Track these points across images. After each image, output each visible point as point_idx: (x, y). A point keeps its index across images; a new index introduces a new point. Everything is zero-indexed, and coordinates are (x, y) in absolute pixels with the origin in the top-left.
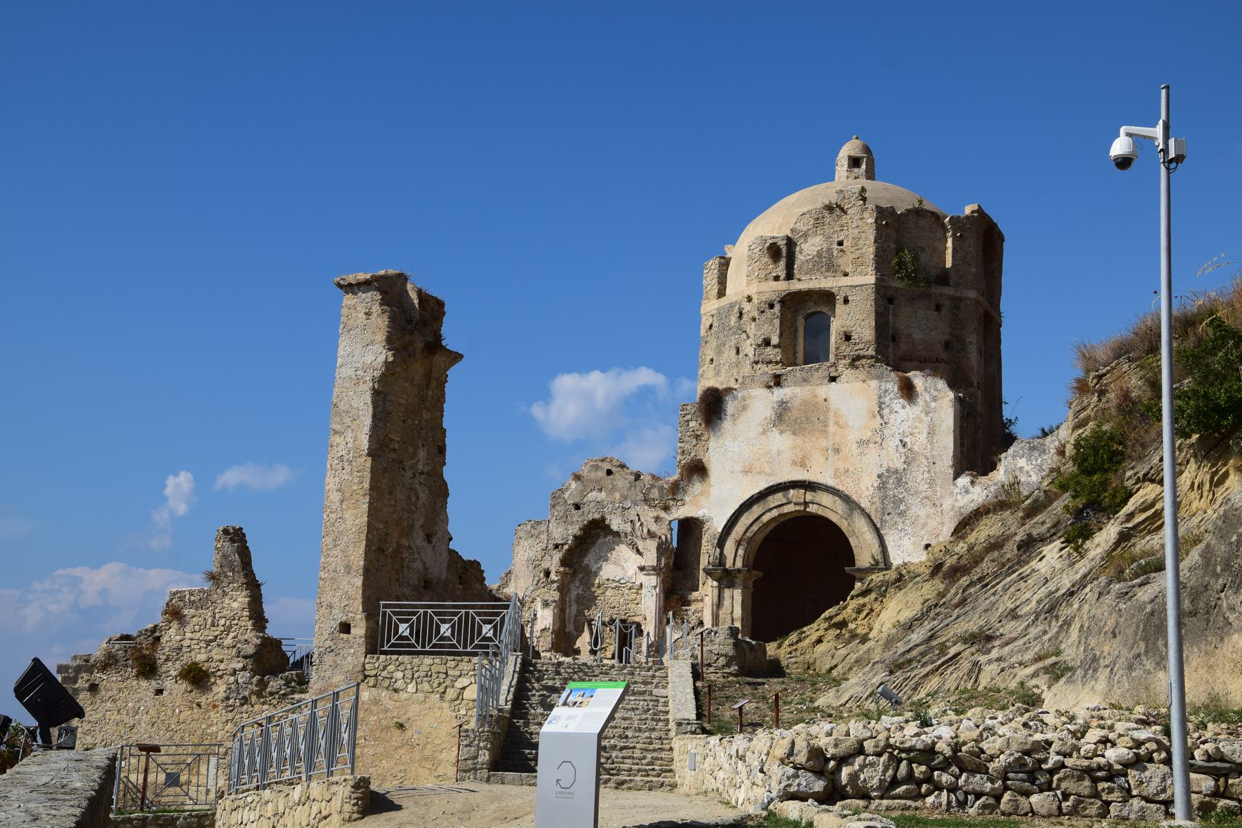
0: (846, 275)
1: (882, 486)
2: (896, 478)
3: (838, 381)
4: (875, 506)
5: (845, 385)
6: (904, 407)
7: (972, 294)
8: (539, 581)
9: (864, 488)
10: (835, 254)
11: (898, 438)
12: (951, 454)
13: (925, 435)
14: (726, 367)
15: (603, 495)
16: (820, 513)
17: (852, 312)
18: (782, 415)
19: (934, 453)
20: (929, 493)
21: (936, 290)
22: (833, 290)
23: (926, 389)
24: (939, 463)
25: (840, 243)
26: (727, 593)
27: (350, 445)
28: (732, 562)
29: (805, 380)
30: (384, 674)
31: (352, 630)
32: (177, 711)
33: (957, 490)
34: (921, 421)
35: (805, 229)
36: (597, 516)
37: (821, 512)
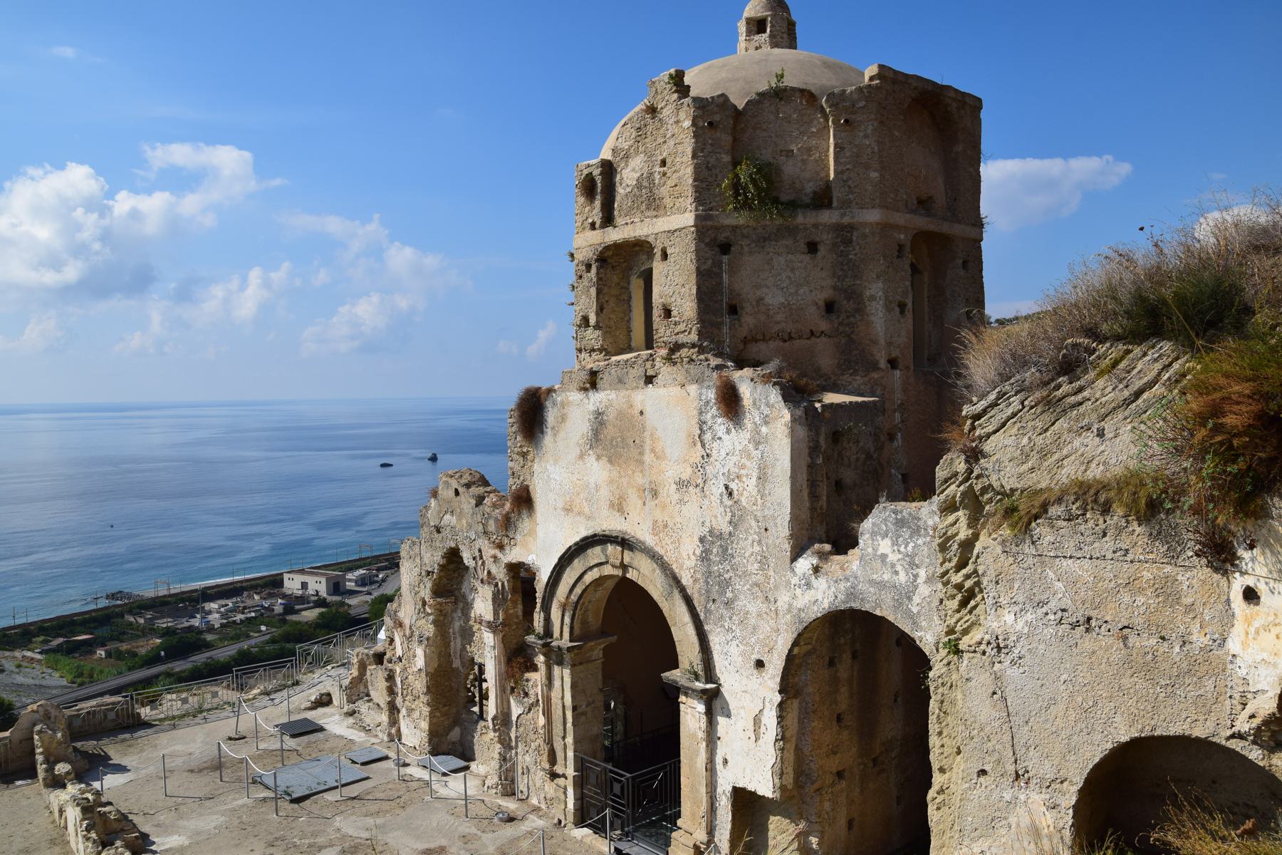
1: (705, 557)
2: (721, 546)
4: (698, 586)
5: (662, 391)
6: (728, 432)
7: (873, 216)
10: (657, 182)
11: (722, 481)
12: (788, 518)
13: (754, 479)
17: (671, 273)
19: (767, 512)
20: (760, 578)
21: (801, 219)
22: (650, 240)
23: (754, 404)
24: (772, 530)
25: (663, 163)
26: (557, 670)
28: (559, 631)
29: (620, 381)
33: (795, 580)
34: (749, 457)
36: (453, 545)
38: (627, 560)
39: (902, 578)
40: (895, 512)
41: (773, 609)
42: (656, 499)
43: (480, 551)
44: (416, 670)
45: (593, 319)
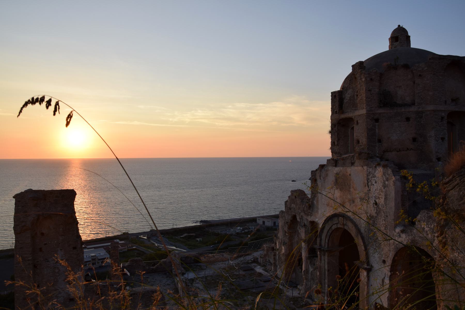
2: (373, 220)
5: (356, 168)
11: (374, 199)
13: (383, 199)
22: (353, 118)
34: (382, 192)
38: (345, 223)
40: (428, 214)
41: (389, 243)
42: (354, 203)
43: (302, 216)
44: (282, 253)
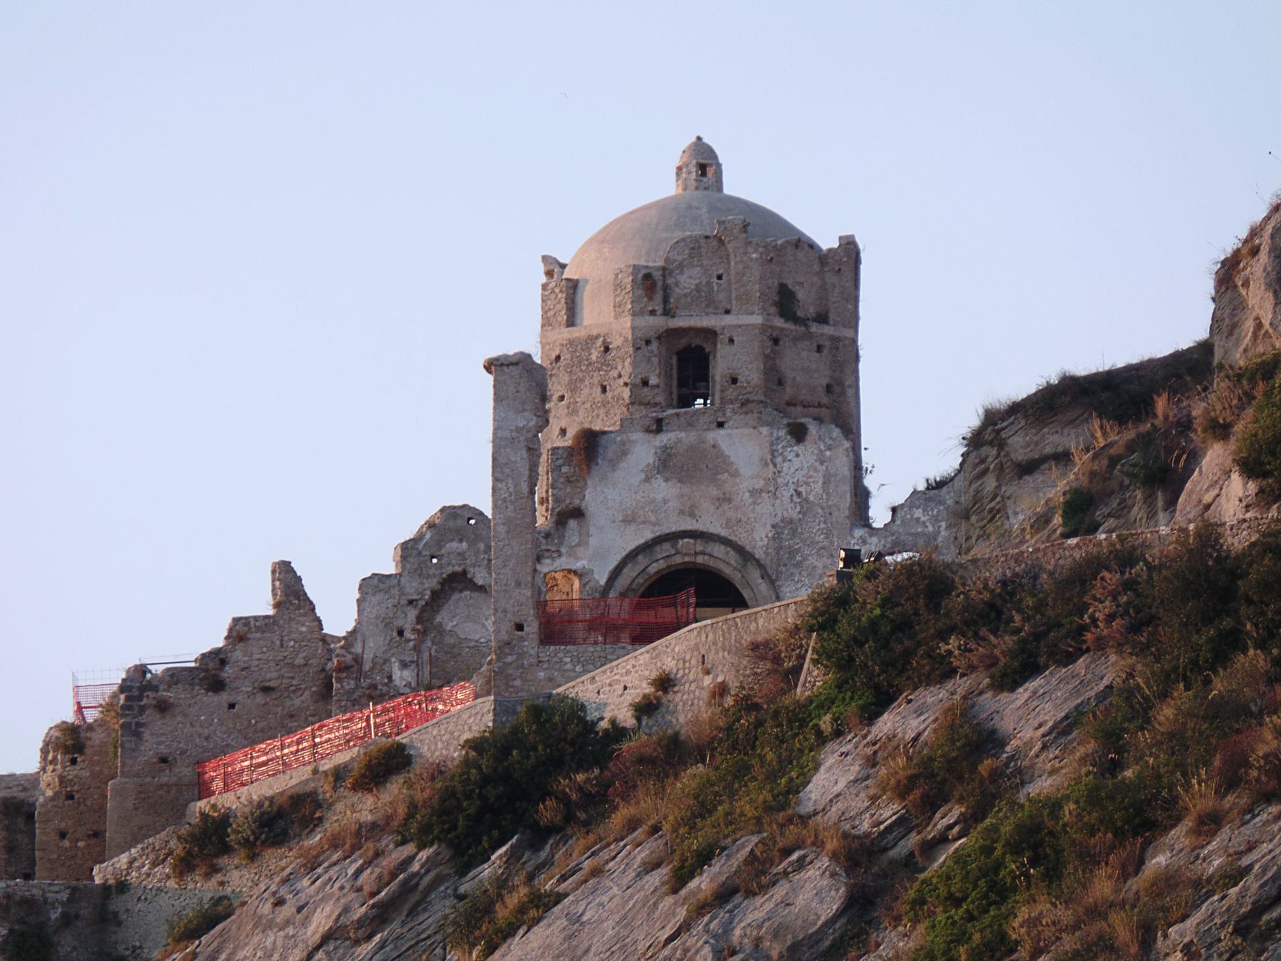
0: (727, 312)
1: (777, 537)
3: (726, 426)
8: (391, 640)
9: (757, 538)
10: (715, 289)
11: (792, 487)
13: (820, 484)
14: (588, 405)
15: (464, 544)
16: (711, 564)
18: (666, 464)
19: (830, 503)
21: (815, 328)
23: (820, 438)
27: (511, 490)
29: (690, 425)
30: (555, 659)
31: (526, 629)
32: (253, 721)
34: (815, 470)
35: (679, 258)
36: (458, 569)
37: (711, 563)
39: (930, 529)
45: (653, 380)
